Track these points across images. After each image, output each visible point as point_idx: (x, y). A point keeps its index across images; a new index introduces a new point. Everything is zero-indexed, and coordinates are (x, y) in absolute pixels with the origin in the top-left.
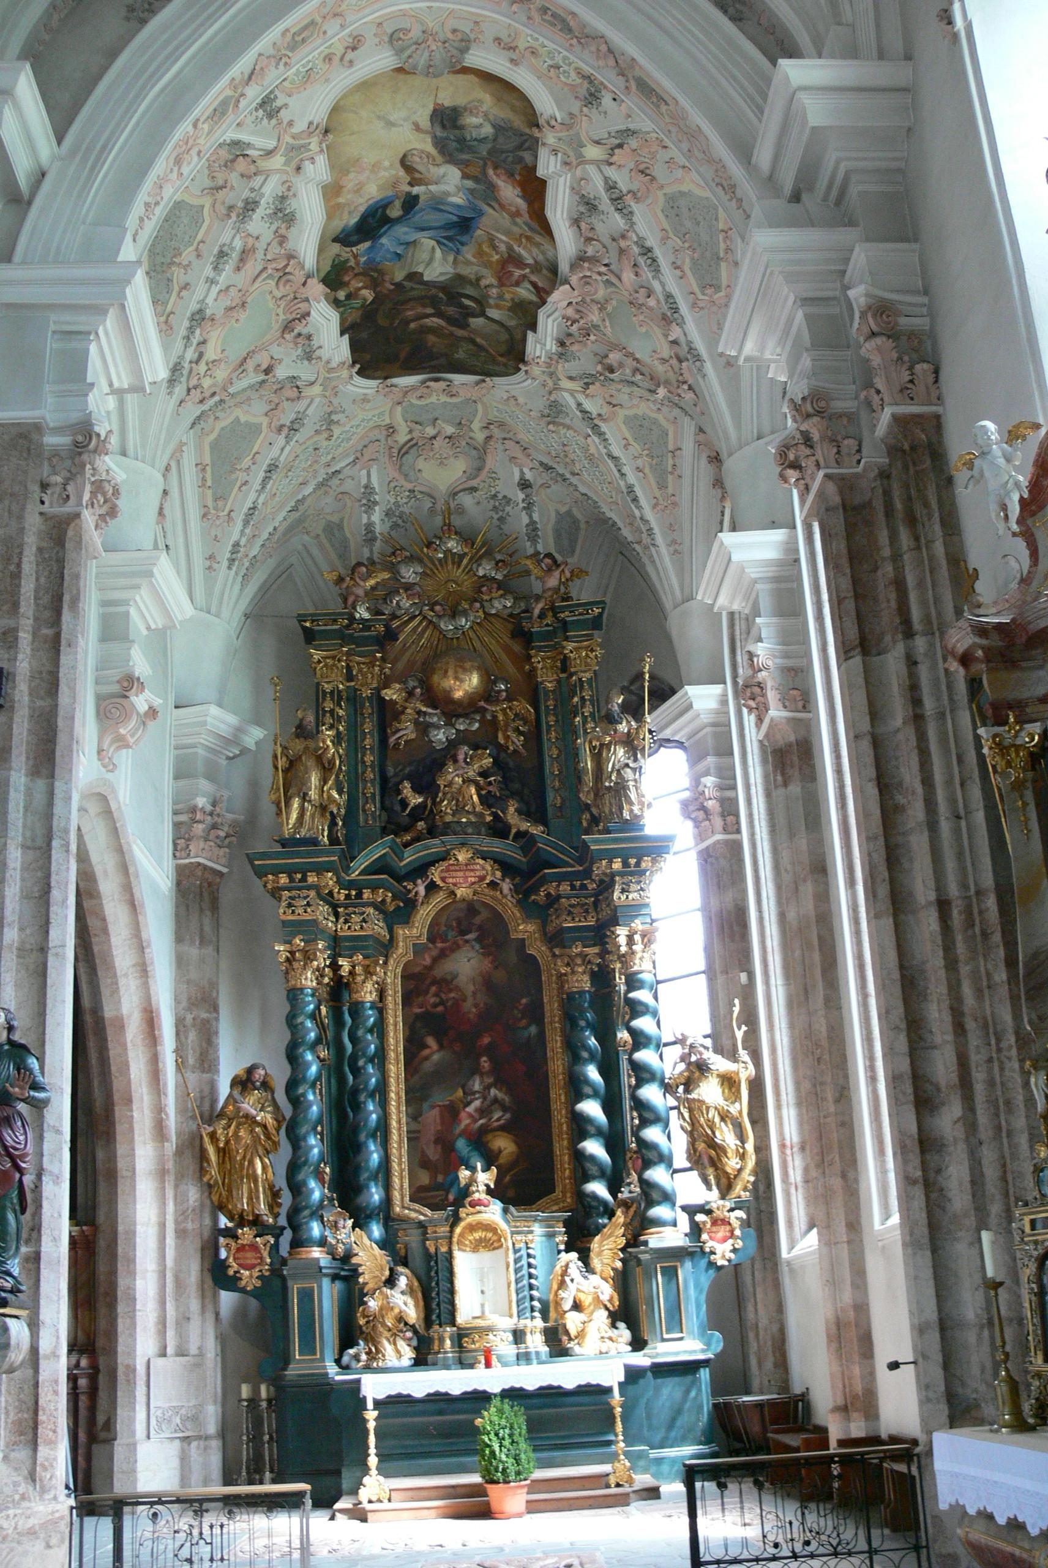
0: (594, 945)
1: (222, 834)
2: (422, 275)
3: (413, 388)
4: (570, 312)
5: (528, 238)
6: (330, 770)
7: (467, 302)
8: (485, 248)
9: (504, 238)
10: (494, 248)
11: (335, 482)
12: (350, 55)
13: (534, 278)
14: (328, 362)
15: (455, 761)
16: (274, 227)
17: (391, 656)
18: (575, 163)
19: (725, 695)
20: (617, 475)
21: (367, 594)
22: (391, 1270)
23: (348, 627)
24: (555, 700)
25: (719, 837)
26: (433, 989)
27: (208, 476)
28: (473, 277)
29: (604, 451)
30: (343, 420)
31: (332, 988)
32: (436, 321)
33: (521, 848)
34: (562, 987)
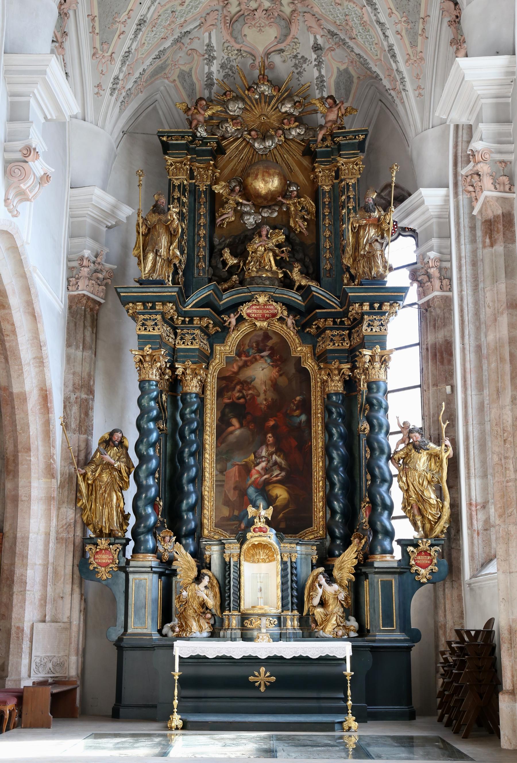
0: (347, 362)
1: (100, 276)
6: (175, 236)
11: (186, 40)
15: (260, 236)
17: (221, 164)
19: (448, 196)
21: (205, 121)
22: (199, 571)
23: (192, 142)
24: (330, 197)
25: (437, 293)
26: (238, 387)
27: (97, 25)
31: (171, 383)
33: (301, 296)
34: (324, 389)
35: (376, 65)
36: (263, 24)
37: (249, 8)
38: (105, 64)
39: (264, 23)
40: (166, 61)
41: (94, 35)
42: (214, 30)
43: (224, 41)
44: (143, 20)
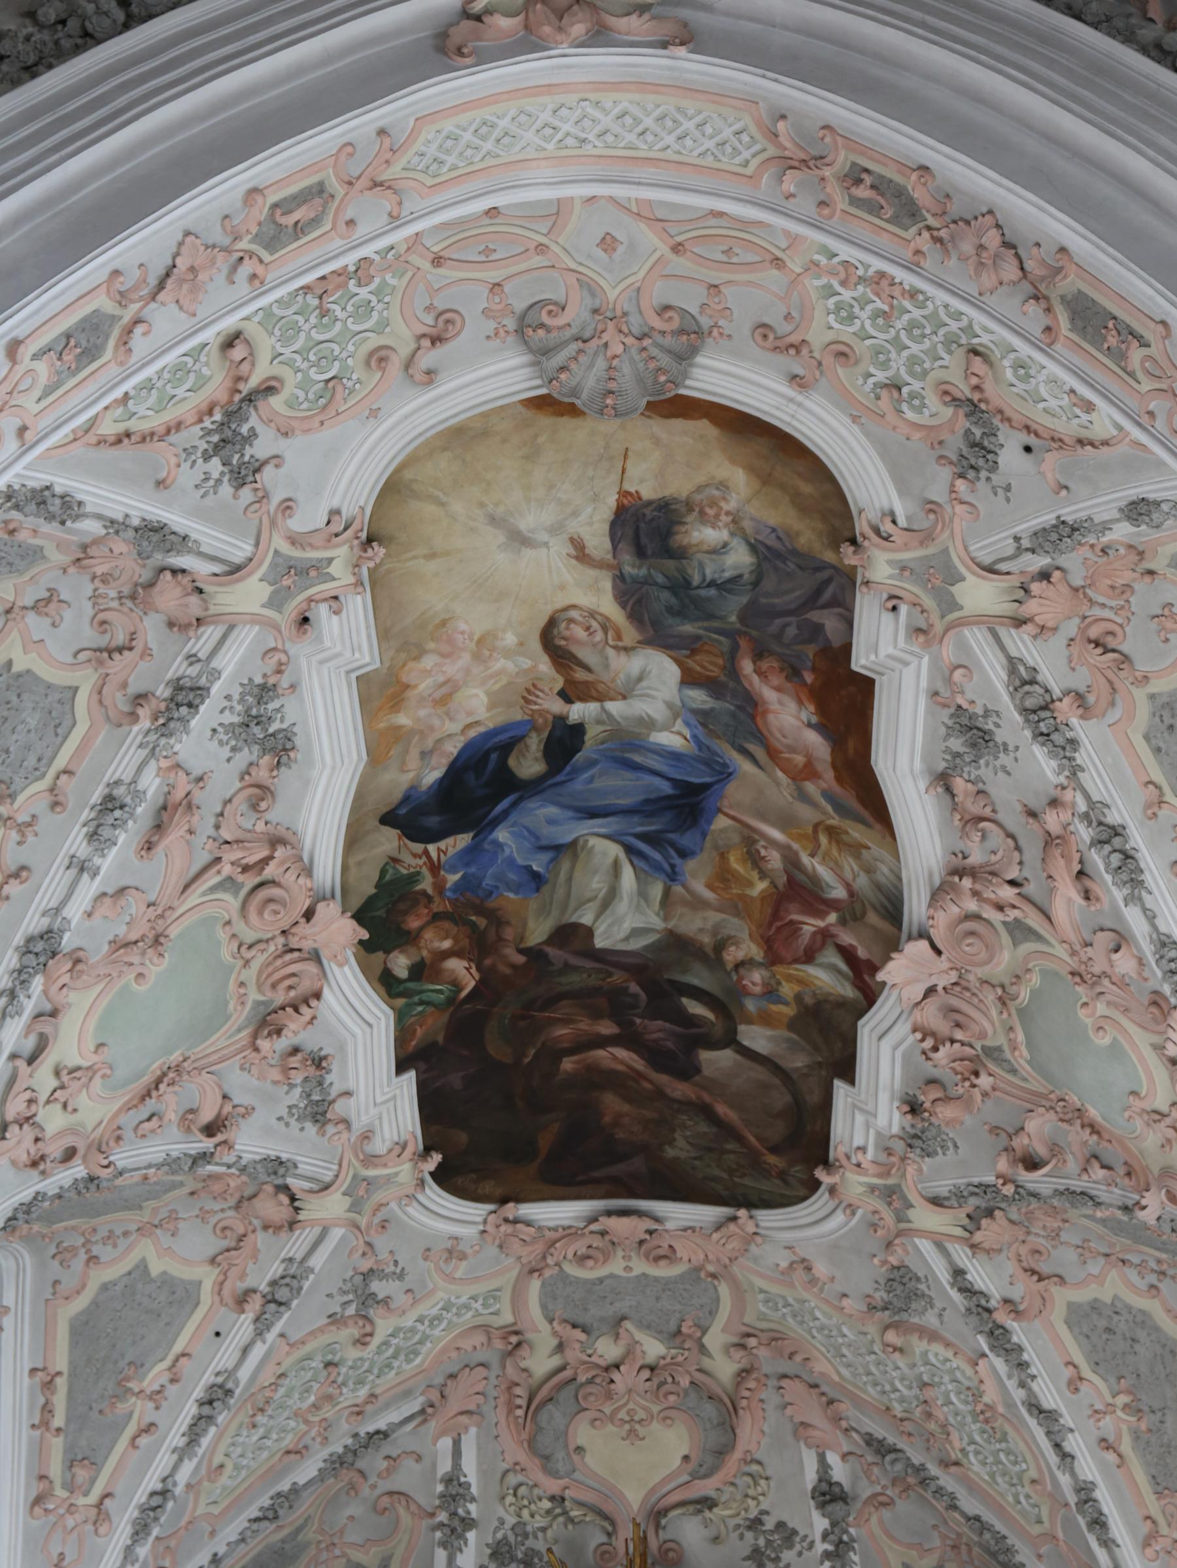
2: (589, 932)
3: (569, 1233)
4: (931, 1016)
5: (832, 832)
7: (695, 1008)
8: (735, 863)
9: (776, 834)
10: (755, 860)
11: (373, 1462)
12: (428, 358)
13: (847, 938)
14: (366, 1136)
16: (244, 757)
18: (939, 627)
20: (1053, 1458)
28: (706, 940)
29: (1019, 1395)
30: (401, 1300)
32: (622, 1057)
35: (1039, 1556)
36: (641, 1414)
37: (593, 1359)
38: (75, 1534)
39: (645, 1409)
40: (298, 1530)
41: (48, 1435)
42: (473, 1430)
43: (505, 1466)
44: (221, 1386)
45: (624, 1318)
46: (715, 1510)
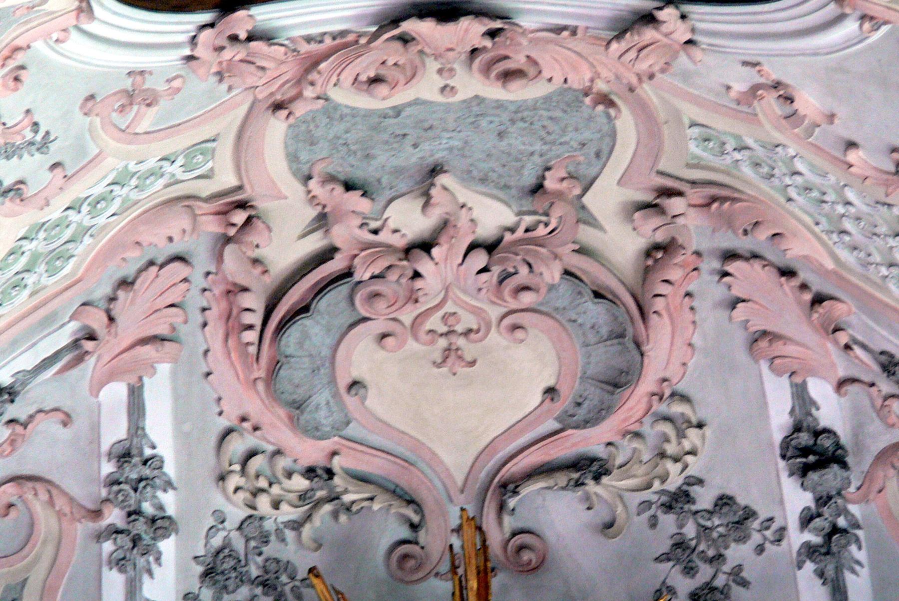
36: (468, 321)
37: (383, 237)
39: (476, 312)
42: (164, 368)
43: (224, 423)
45: (435, 171)
46: (605, 480)
